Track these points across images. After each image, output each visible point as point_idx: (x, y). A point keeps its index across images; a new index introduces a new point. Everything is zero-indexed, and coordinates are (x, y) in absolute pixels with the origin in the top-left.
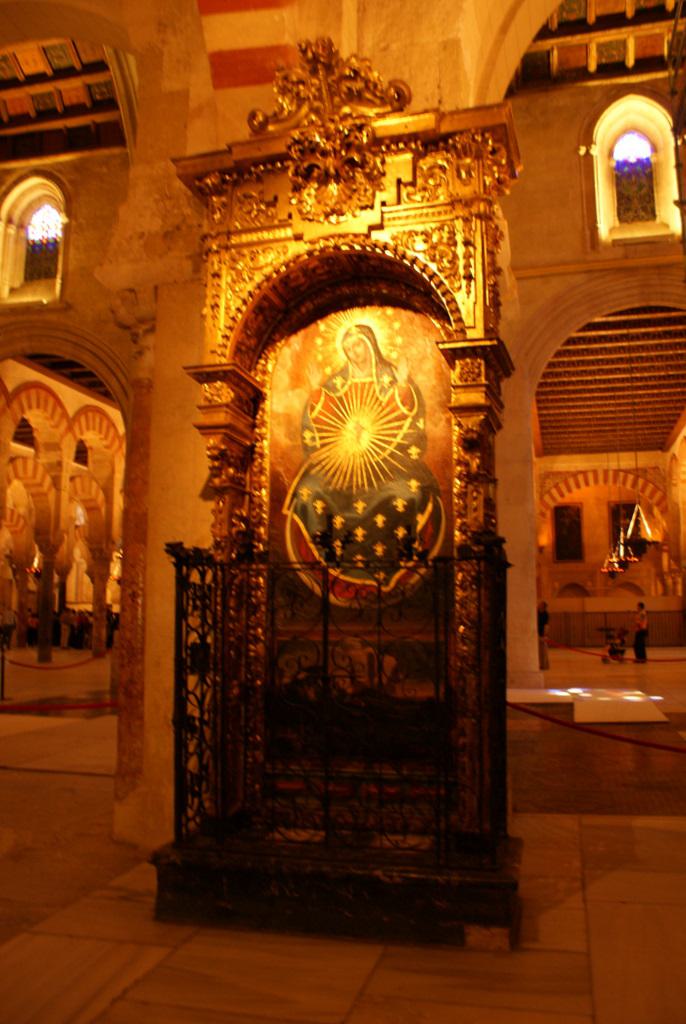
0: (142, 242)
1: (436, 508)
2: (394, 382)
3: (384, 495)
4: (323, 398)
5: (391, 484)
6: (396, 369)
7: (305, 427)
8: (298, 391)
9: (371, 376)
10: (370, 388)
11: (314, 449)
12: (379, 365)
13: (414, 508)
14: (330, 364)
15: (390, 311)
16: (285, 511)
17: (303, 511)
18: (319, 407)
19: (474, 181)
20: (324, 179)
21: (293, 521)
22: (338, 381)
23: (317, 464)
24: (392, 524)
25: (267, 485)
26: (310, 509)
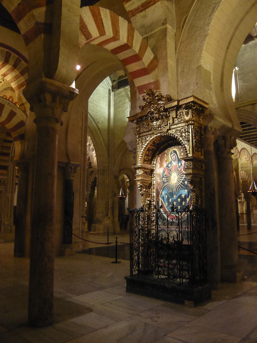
0: (133, 130)
2: (181, 165)
17: (163, 198)
19: (189, 115)
20: (157, 120)
22: (170, 165)
24: (182, 201)
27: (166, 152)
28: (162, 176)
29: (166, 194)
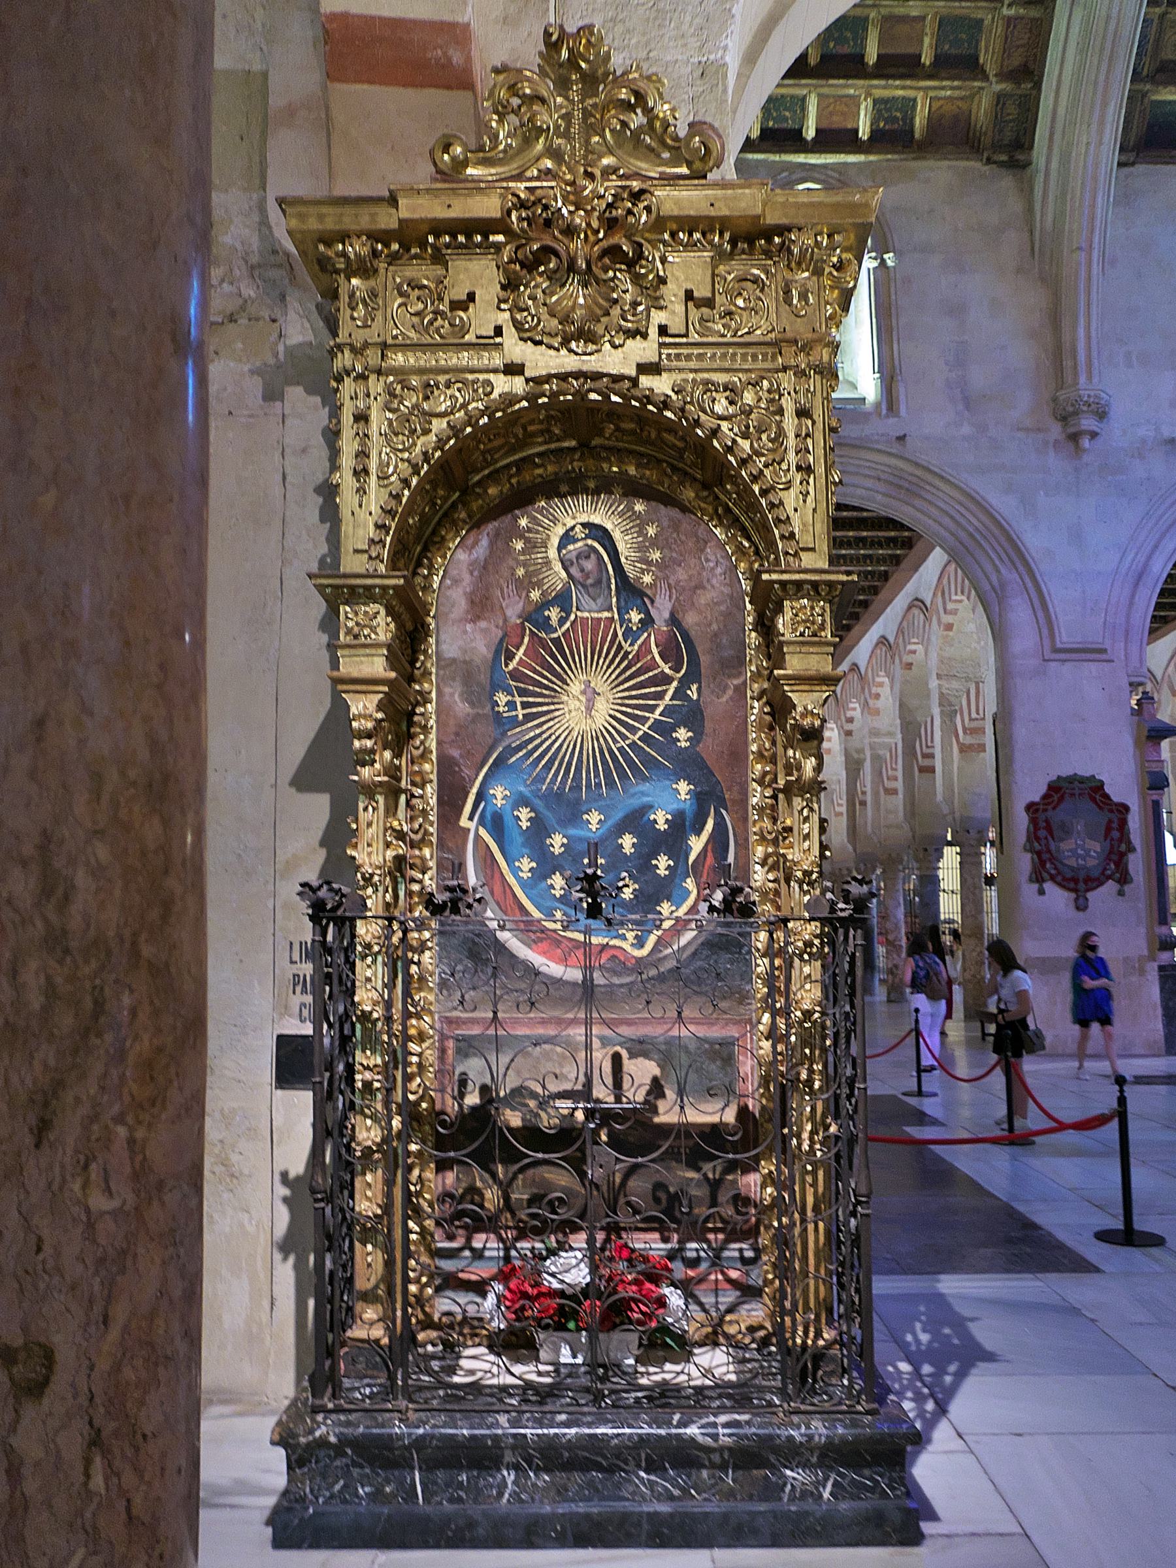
1: (720, 825)
3: (635, 802)
4: (526, 640)
5: (646, 787)
6: (652, 602)
8: (483, 624)
9: (610, 609)
10: (607, 628)
11: (514, 722)
12: (624, 594)
13: (681, 827)
14: (539, 584)
16: (464, 822)
18: (520, 653)
21: (477, 836)
22: (554, 614)
23: (519, 748)
25: (434, 777)
26: (508, 820)
27: (523, 522)
29: (522, 801)
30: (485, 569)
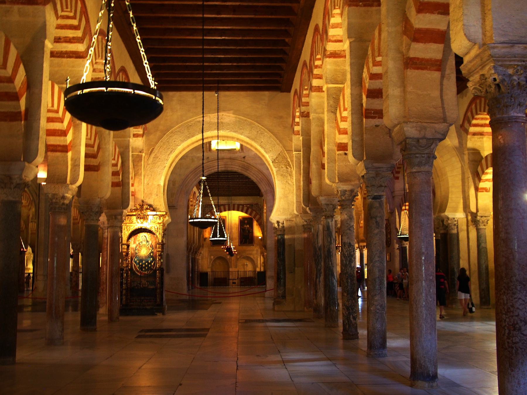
7: (136, 250)
15: (149, 233)
17: (136, 262)
28: (135, 249)
30: (134, 239)
